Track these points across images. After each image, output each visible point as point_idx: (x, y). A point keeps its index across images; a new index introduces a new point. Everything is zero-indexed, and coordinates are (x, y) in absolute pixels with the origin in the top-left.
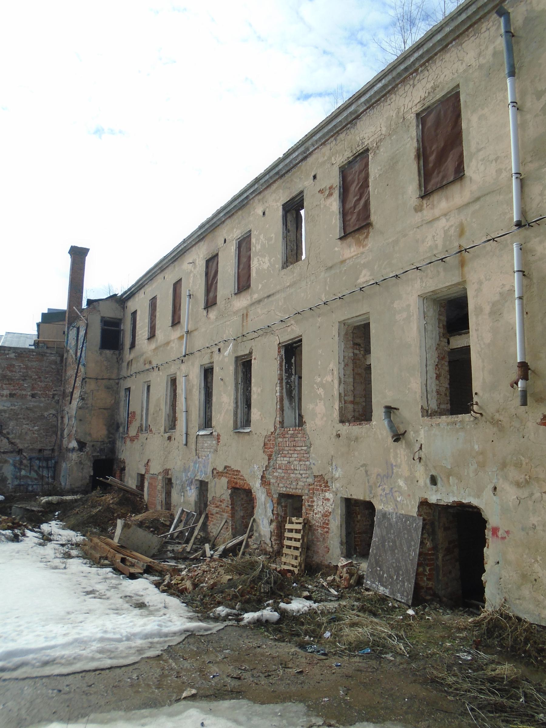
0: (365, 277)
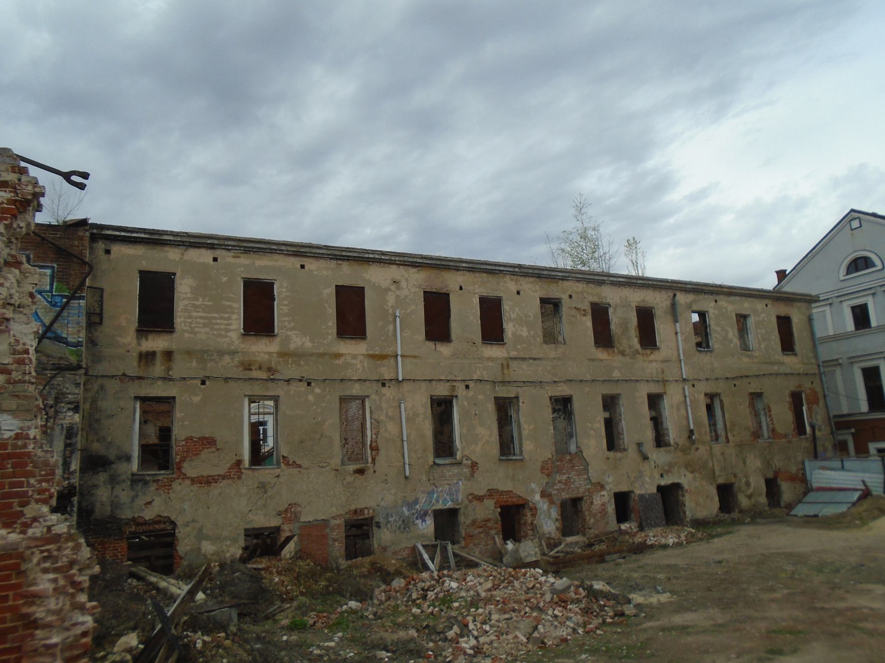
0: (616, 374)
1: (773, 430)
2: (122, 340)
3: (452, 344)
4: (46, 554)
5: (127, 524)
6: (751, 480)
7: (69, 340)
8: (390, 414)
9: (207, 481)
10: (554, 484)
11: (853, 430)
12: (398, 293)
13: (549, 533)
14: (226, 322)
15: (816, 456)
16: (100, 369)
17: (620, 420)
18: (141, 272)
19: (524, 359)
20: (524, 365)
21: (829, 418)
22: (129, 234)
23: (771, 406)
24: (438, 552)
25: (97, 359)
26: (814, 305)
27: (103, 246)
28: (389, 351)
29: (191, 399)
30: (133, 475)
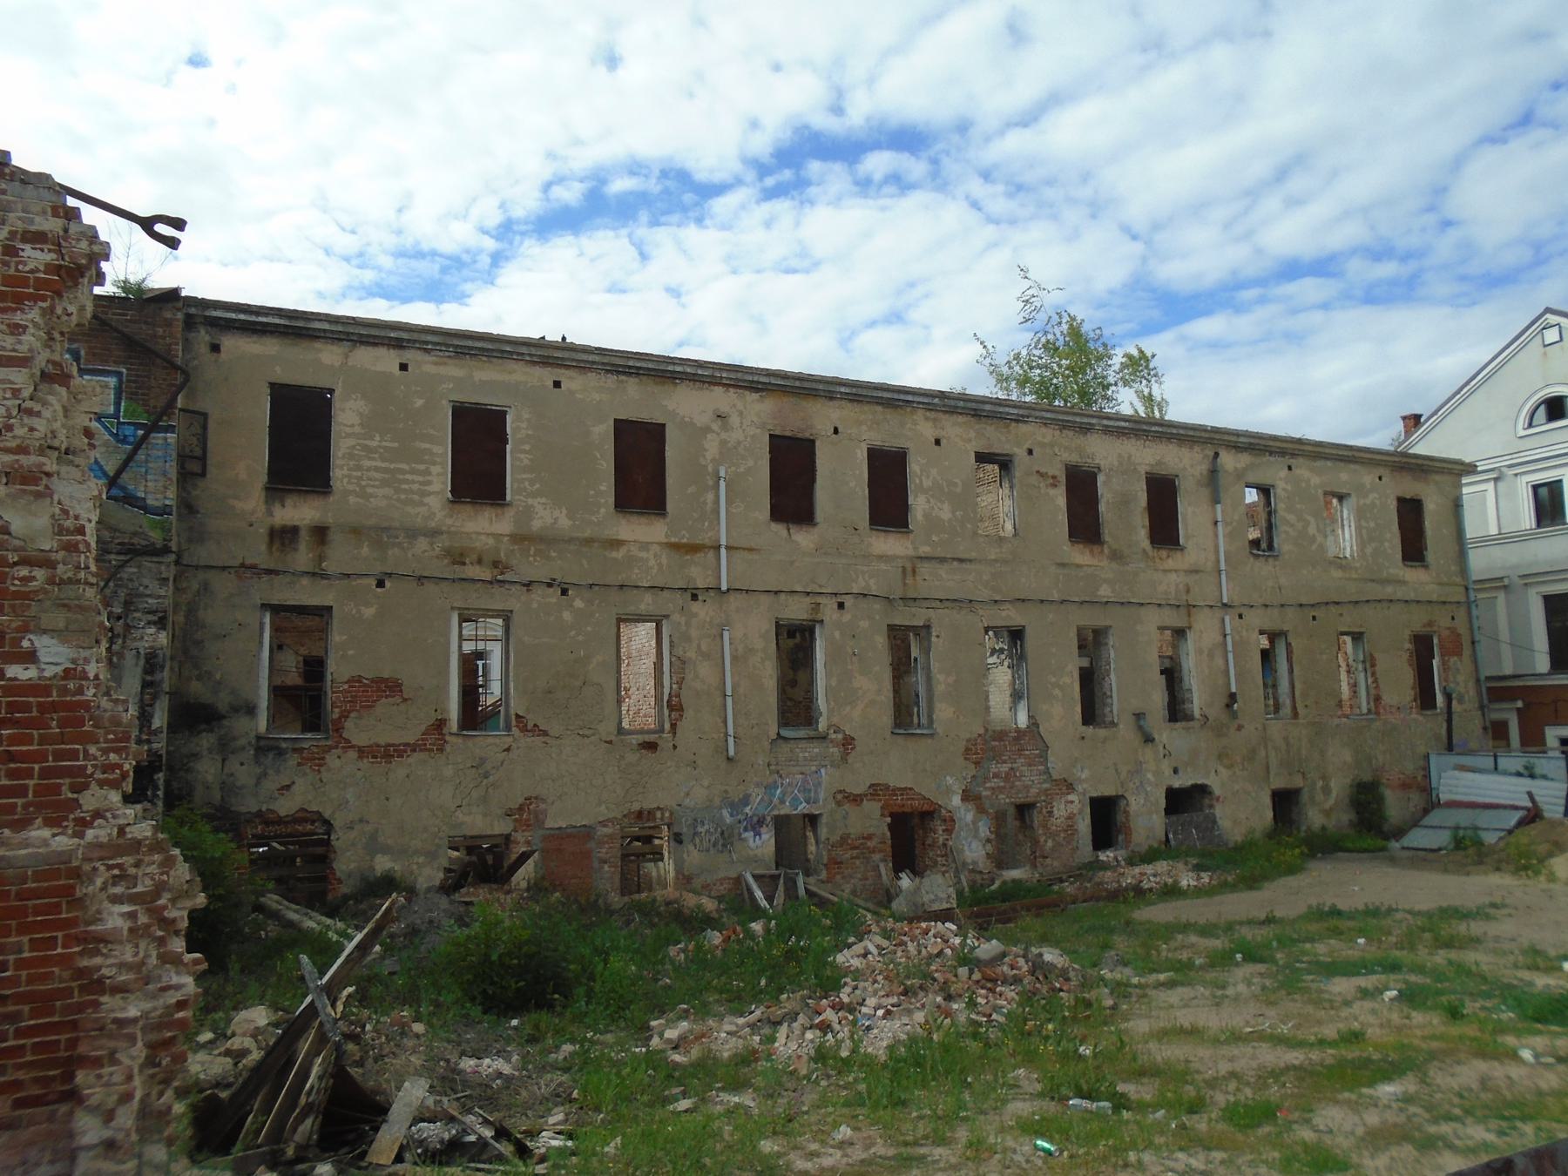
0: (1105, 592)
1: (1378, 699)
2: (239, 505)
3: (816, 530)
4: (116, 872)
5: (248, 821)
6: (1332, 784)
7: (149, 502)
8: (704, 648)
9: (388, 753)
10: (986, 779)
11: (1520, 704)
12: (724, 435)
13: (974, 863)
14: (421, 479)
15: (1450, 748)
16: (203, 554)
17: (1108, 672)
18: (272, 385)
19: (942, 560)
20: (943, 571)
21: (1478, 680)
22: (253, 318)
23: (1376, 655)
24: (781, 888)
25: (197, 535)
26: (1465, 480)
27: (207, 338)
28: (705, 538)
29: (359, 611)
30: (259, 738)
